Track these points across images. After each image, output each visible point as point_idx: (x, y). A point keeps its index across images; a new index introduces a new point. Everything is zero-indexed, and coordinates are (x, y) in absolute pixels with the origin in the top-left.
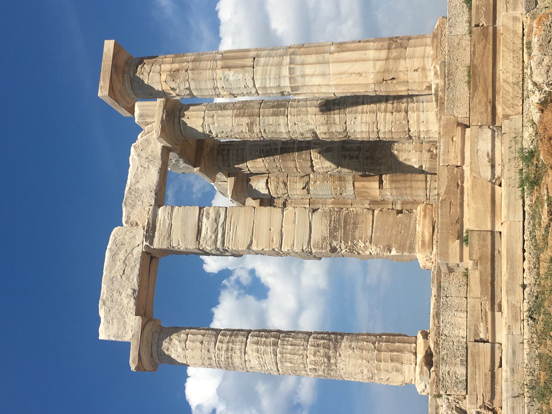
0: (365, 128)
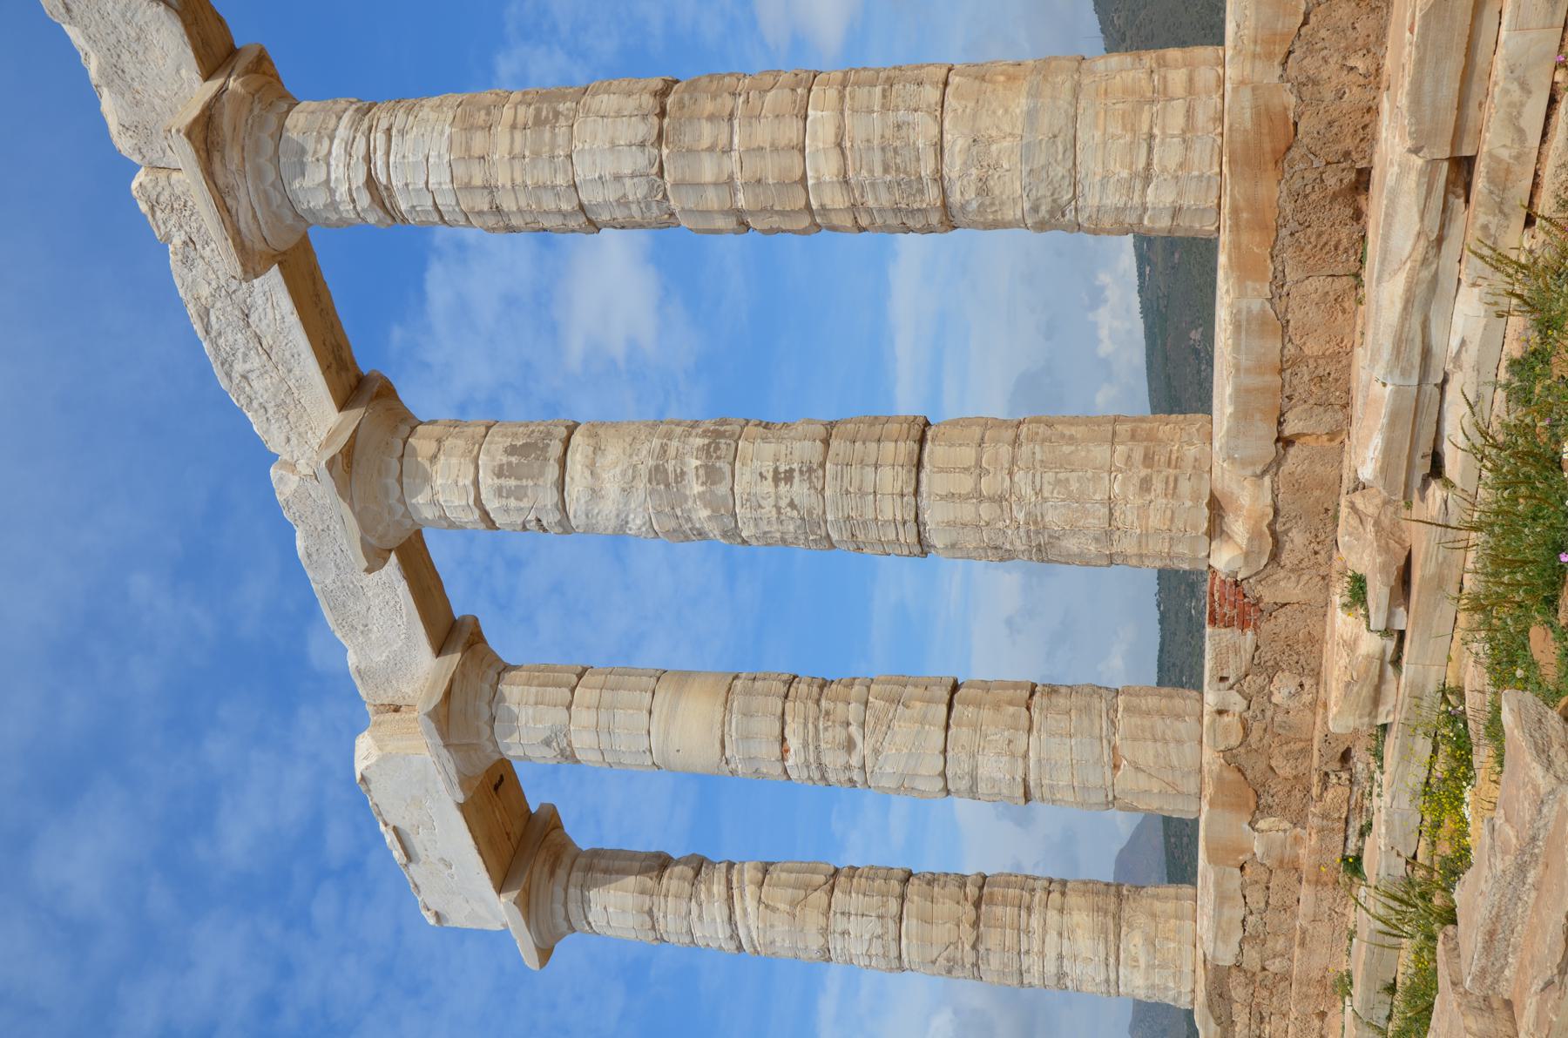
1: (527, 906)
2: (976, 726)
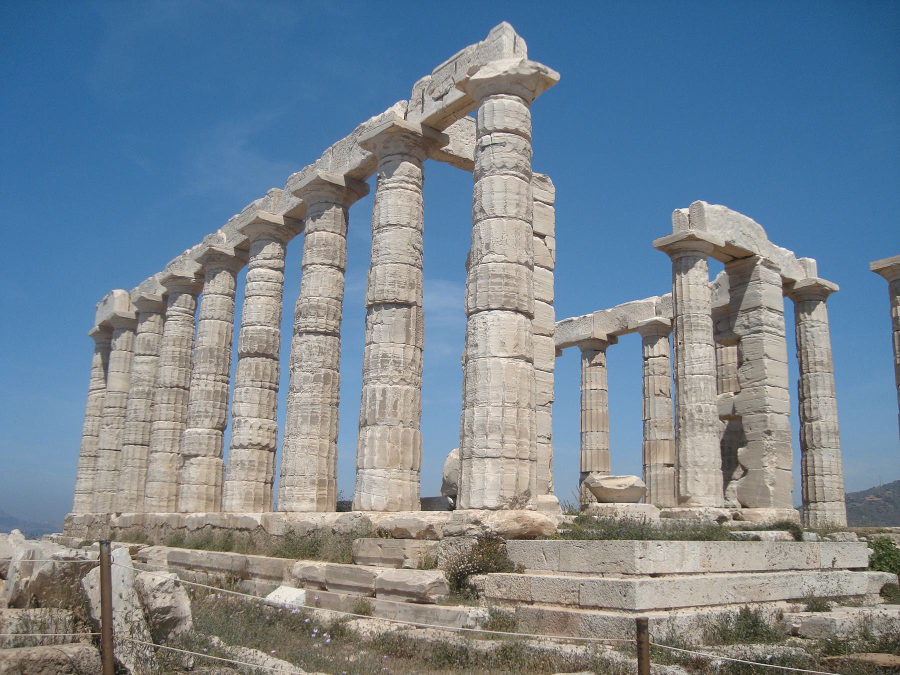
0: (825, 464)
1: (96, 333)
2: (109, 457)
